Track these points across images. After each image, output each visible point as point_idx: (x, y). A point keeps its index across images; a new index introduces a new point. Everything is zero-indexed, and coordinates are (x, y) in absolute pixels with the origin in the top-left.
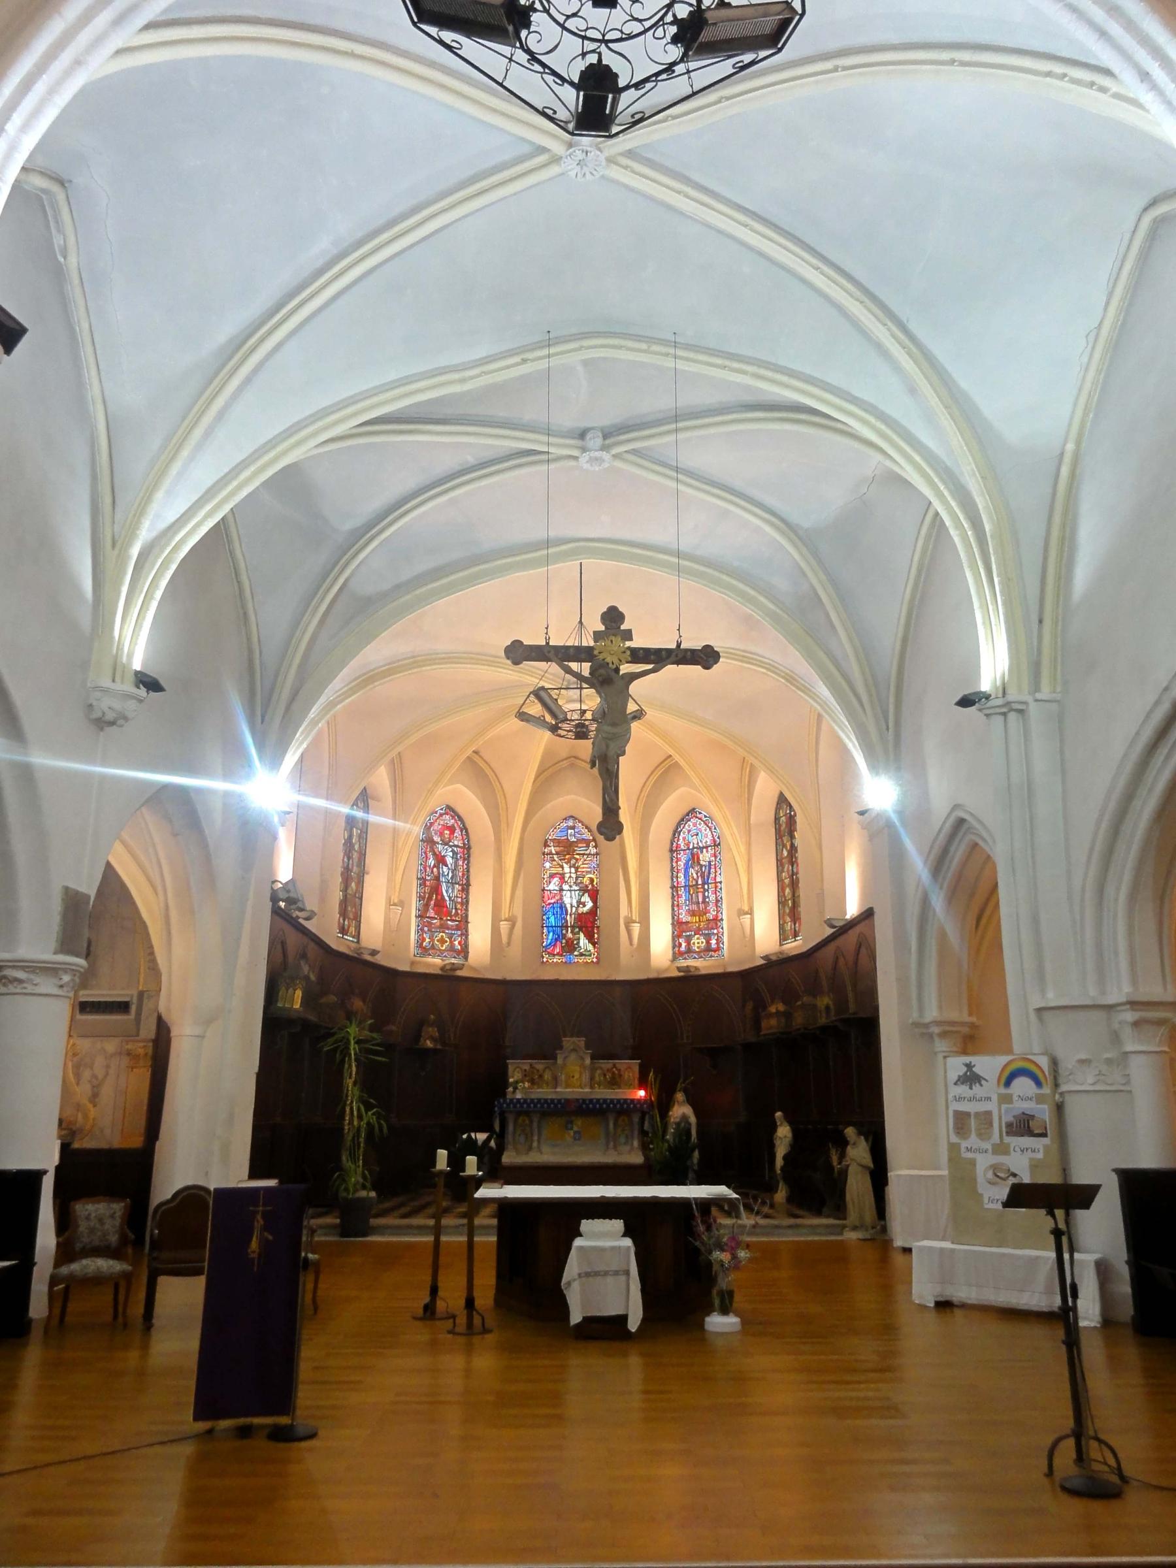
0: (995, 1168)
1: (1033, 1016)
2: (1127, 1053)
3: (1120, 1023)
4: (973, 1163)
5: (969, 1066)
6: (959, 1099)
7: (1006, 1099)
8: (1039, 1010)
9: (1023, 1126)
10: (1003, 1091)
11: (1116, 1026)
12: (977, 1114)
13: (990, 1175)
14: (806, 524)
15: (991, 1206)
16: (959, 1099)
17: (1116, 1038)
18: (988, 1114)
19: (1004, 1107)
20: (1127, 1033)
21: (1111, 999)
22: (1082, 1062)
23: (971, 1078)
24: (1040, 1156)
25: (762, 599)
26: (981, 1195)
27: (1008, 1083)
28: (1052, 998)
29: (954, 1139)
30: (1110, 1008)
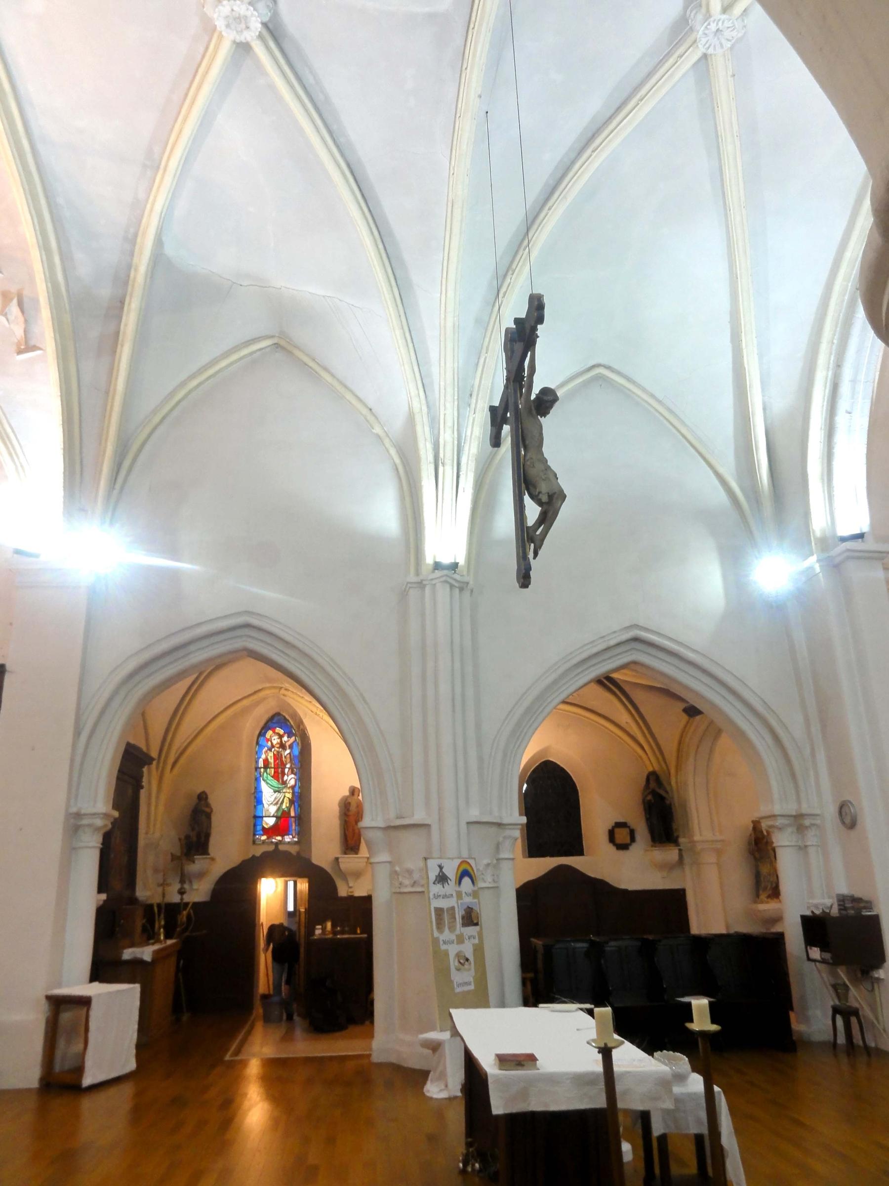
0: (458, 955)
1: (463, 826)
2: (498, 860)
3: (505, 838)
4: (446, 953)
5: (441, 867)
6: (437, 897)
7: (459, 895)
8: (468, 823)
9: (470, 918)
10: (458, 889)
11: (501, 839)
12: (448, 909)
13: (457, 963)
14: (169, 250)
15: (458, 990)
16: (437, 897)
17: (498, 847)
18: (453, 908)
19: (460, 902)
20: (508, 843)
21: (506, 821)
22: (488, 865)
23: (442, 878)
24: (476, 941)
25: (57, 260)
26: (452, 982)
27: (460, 883)
28: (474, 814)
29: (436, 934)
30: (499, 825)
